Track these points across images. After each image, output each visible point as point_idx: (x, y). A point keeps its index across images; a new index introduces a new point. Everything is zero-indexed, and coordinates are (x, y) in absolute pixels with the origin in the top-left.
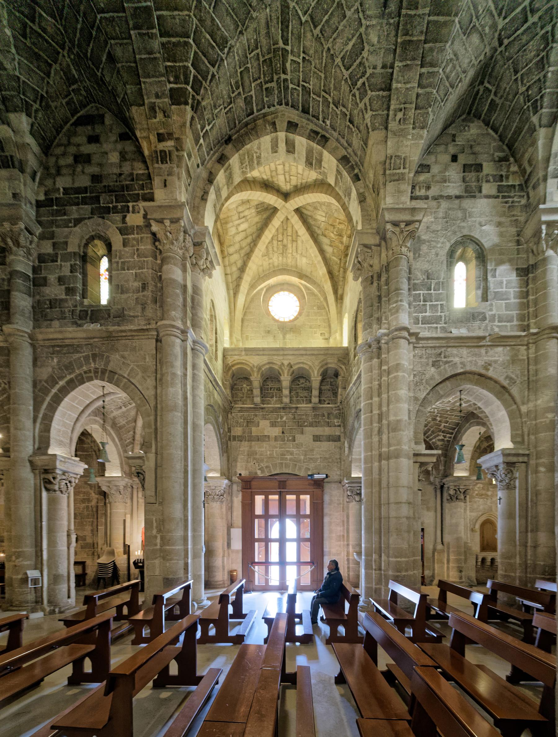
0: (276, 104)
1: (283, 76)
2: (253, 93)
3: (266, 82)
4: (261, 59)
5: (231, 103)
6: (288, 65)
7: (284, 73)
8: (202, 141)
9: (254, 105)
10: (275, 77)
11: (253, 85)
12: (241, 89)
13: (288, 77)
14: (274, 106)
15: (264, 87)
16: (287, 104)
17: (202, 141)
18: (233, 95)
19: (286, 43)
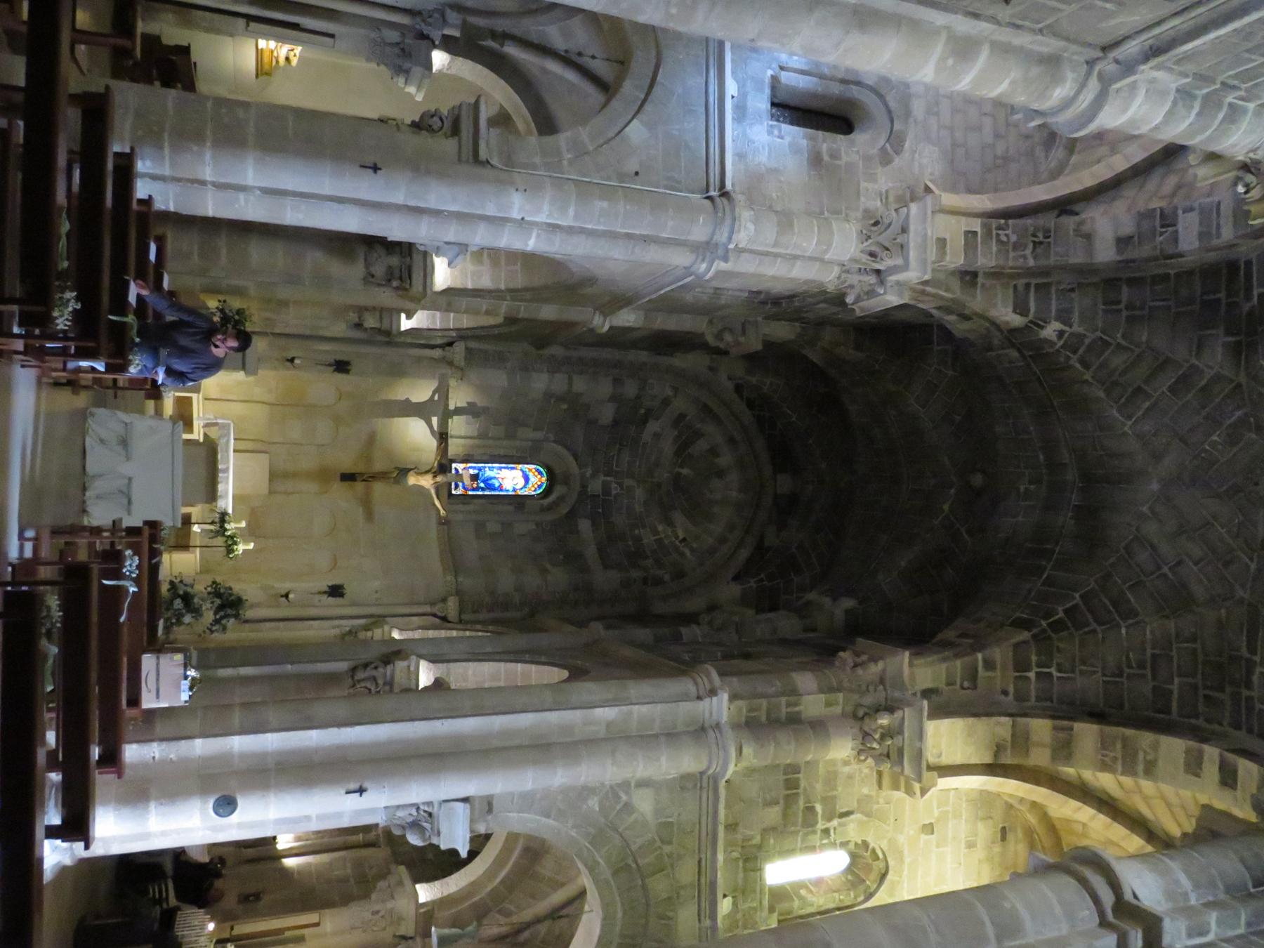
0: (1225, 723)
1: (1245, 693)
2: (1175, 687)
3: (1206, 687)
4: (1201, 658)
5: (1121, 675)
6: (1255, 678)
7: (1249, 685)
8: (1032, 675)
9: (1174, 705)
10: (1228, 689)
11: (1176, 680)
12: (1148, 672)
13: (1255, 694)
14: (1220, 724)
15: (1201, 692)
16: (1250, 731)
17: (1032, 675)
18: (1127, 671)
19: (1252, 650)
